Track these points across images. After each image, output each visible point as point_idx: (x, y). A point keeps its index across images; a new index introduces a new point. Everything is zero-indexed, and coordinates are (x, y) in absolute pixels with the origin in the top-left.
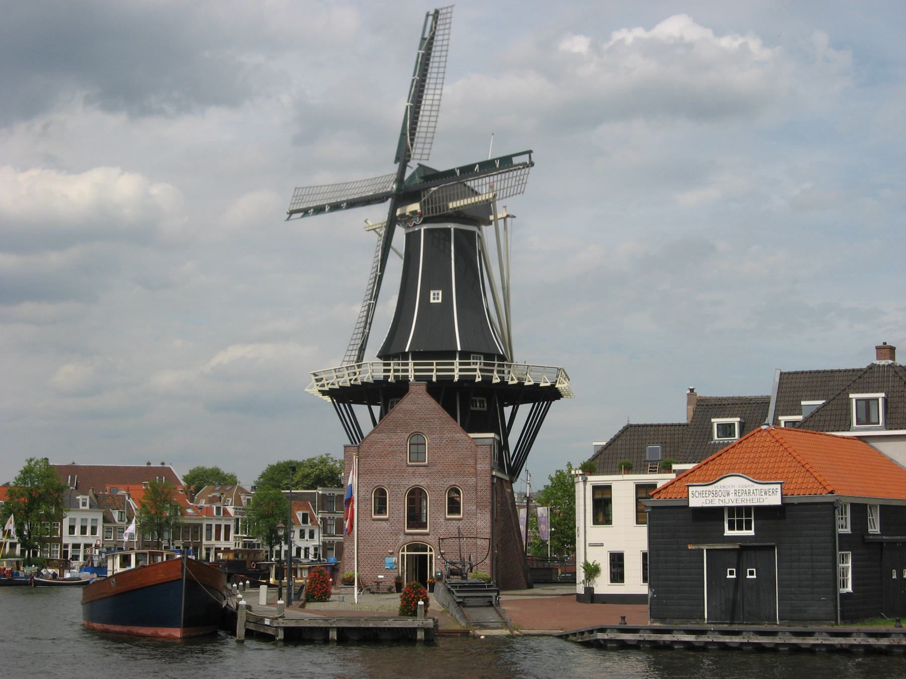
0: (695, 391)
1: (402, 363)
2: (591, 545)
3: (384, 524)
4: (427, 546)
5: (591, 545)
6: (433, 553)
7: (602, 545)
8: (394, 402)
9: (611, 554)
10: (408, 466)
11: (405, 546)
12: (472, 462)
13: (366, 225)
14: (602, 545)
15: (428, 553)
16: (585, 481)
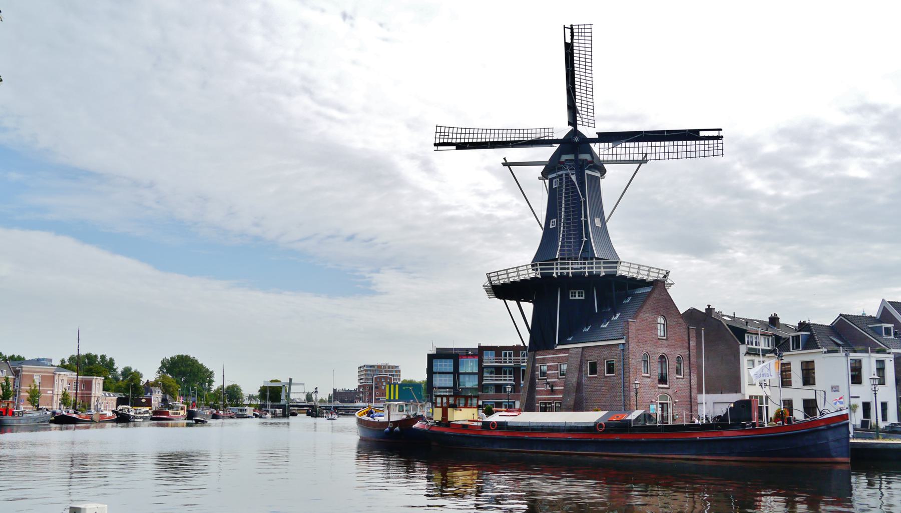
0: (711, 307)
1: (539, 263)
2: (852, 397)
3: (648, 380)
4: (667, 397)
5: (852, 397)
6: (671, 402)
7: (858, 397)
8: (575, 293)
9: (863, 403)
10: (659, 339)
11: (658, 396)
12: (686, 338)
13: (504, 162)
14: (858, 397)
15: (669, 402)
16: (846, 355)
